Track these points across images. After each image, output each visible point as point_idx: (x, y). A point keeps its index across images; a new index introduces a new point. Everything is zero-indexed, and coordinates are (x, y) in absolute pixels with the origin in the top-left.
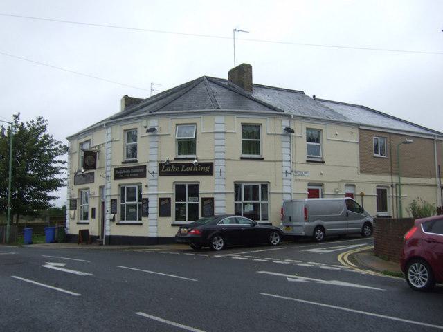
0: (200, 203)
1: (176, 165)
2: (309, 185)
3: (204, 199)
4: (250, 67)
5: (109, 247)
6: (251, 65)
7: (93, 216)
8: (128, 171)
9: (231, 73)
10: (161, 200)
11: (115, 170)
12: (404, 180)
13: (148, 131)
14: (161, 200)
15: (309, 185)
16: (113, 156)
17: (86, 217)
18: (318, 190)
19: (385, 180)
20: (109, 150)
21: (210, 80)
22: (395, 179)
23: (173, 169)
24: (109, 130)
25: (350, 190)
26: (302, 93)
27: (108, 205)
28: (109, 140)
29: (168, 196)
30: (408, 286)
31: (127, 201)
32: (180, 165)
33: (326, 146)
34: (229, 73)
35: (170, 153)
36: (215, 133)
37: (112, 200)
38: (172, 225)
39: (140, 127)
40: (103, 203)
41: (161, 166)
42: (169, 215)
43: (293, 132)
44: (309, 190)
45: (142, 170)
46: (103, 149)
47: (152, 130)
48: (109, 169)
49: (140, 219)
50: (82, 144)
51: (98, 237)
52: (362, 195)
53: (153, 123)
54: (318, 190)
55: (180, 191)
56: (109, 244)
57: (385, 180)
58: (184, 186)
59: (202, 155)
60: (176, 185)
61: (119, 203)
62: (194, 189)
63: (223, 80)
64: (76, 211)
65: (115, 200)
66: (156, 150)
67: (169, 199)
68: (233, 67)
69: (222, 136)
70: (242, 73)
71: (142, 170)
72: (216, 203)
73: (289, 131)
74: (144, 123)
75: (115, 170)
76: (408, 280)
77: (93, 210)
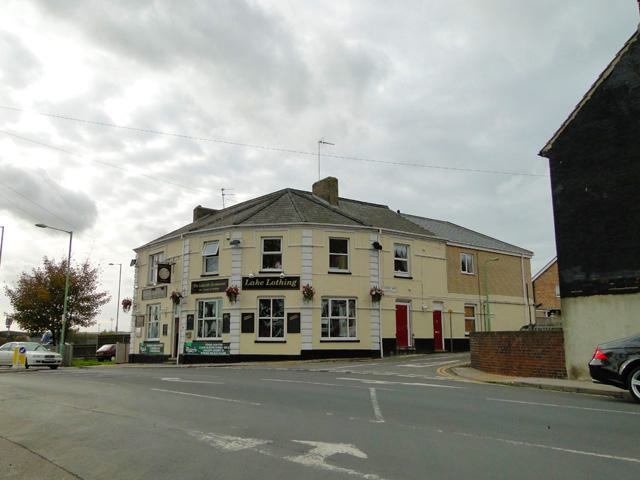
0: (285, 318)
1: (260, 279)
2: (397, 300)
3: (289, 315)
4: (336, 181)
5: (181, 366)
6: (338, 178)
7: (165, 333)
8: (208, 285)
9: (315, 186)
10: (244, 315)
11: (193, 283)
12: (492, 298)
13: (231, 244)
14: (244, 315)
15: (397, 300)
16: (189, 271)
17: (278, 331)
18: (406, 307)
19: (473, 298)
20: (186, 263)
21: (294, 192)
22: (483, 298)
23: (257, 283)
24: (187, 242)
25: (438, 308)
26: (387, 207)
27: (183, 322)
28: (187, 252)
29: (251, 312)
30: (631, 396)
31: (333, 315)
32: (265, 279)
33: (413, 263)
34: (314, 186)
35: (254, 268)
36: (302, 246)
37: (188, 316)
38: (256, 342)
39: (222, 241)
40: (177, 320)
41: (244, 279)
42: (252, 331)
43: (380, 248)
44: (397, 306)
45: (224, 284)
46: (178, 262)
47: (236, 243)
48: (185, 282)
49: (219, 336)
50: (152, 256)
51: (170, 356)
52: (451, 312)
53: (237, 235)
54: (406, 307)
55: (264, 302)
56: (184, 363)
57: (473, 298)
58: (269, 301)
59: (286, 269)
60: (261, 300)
61: (196, 320)
62: (278, 305)
63: (308, 193)
64: (144, 328)
65: (192, 316)
66: (241, 262)
67: (253, 314)
68: (317, 181)
69: (310, 250)
70: (330, 185)
71: (224, 284)
72: (303, 319)
73: (377, 246)
74: (227, 235)
75: (193, 283)
76: (632, 392)
77: (165, 327)
